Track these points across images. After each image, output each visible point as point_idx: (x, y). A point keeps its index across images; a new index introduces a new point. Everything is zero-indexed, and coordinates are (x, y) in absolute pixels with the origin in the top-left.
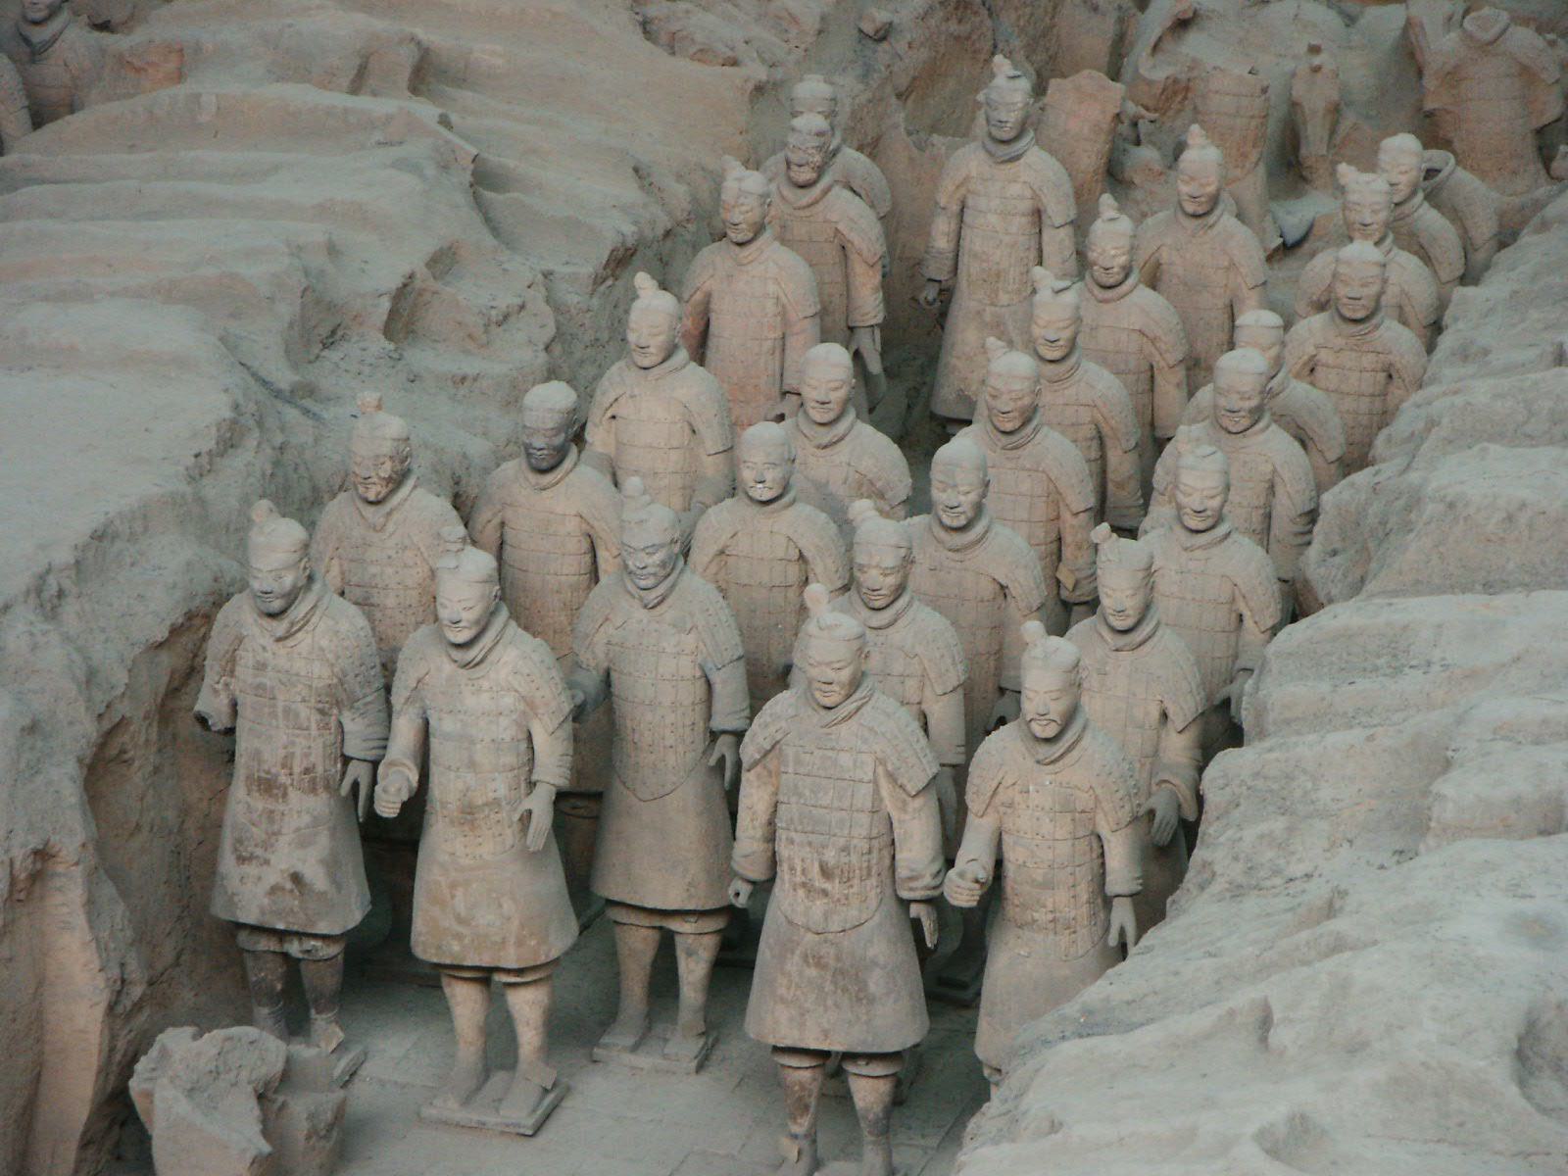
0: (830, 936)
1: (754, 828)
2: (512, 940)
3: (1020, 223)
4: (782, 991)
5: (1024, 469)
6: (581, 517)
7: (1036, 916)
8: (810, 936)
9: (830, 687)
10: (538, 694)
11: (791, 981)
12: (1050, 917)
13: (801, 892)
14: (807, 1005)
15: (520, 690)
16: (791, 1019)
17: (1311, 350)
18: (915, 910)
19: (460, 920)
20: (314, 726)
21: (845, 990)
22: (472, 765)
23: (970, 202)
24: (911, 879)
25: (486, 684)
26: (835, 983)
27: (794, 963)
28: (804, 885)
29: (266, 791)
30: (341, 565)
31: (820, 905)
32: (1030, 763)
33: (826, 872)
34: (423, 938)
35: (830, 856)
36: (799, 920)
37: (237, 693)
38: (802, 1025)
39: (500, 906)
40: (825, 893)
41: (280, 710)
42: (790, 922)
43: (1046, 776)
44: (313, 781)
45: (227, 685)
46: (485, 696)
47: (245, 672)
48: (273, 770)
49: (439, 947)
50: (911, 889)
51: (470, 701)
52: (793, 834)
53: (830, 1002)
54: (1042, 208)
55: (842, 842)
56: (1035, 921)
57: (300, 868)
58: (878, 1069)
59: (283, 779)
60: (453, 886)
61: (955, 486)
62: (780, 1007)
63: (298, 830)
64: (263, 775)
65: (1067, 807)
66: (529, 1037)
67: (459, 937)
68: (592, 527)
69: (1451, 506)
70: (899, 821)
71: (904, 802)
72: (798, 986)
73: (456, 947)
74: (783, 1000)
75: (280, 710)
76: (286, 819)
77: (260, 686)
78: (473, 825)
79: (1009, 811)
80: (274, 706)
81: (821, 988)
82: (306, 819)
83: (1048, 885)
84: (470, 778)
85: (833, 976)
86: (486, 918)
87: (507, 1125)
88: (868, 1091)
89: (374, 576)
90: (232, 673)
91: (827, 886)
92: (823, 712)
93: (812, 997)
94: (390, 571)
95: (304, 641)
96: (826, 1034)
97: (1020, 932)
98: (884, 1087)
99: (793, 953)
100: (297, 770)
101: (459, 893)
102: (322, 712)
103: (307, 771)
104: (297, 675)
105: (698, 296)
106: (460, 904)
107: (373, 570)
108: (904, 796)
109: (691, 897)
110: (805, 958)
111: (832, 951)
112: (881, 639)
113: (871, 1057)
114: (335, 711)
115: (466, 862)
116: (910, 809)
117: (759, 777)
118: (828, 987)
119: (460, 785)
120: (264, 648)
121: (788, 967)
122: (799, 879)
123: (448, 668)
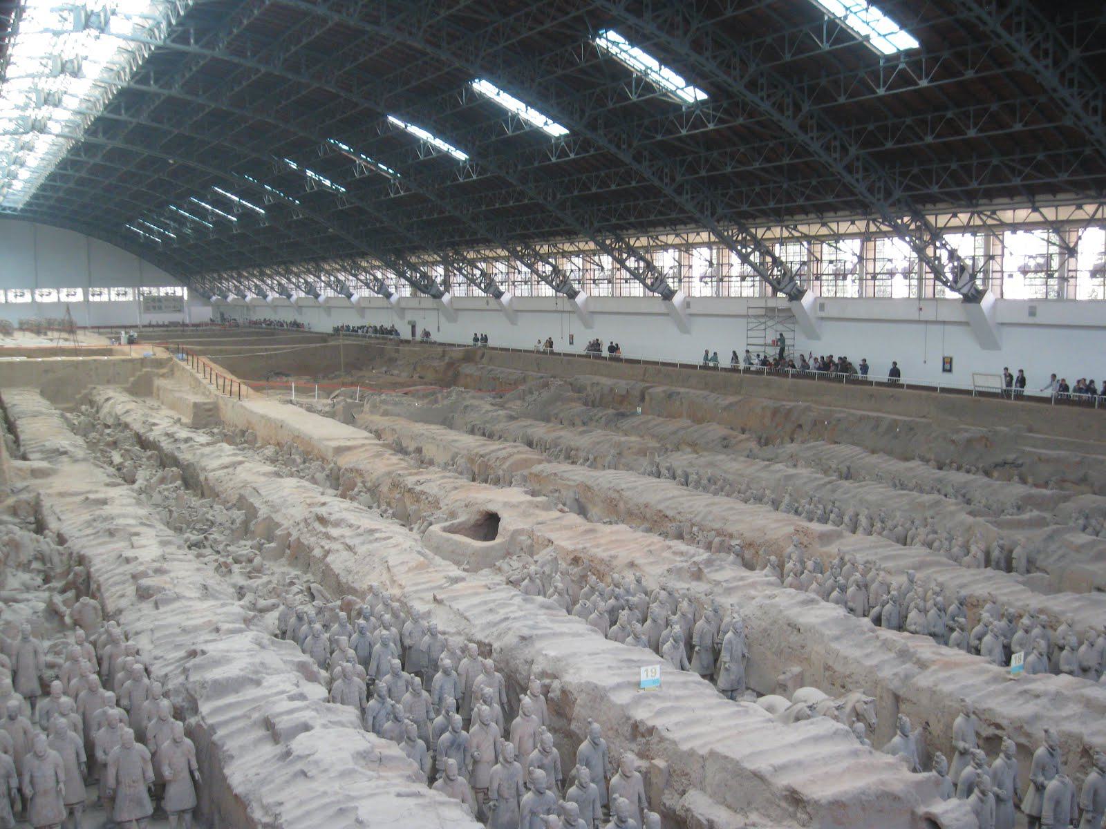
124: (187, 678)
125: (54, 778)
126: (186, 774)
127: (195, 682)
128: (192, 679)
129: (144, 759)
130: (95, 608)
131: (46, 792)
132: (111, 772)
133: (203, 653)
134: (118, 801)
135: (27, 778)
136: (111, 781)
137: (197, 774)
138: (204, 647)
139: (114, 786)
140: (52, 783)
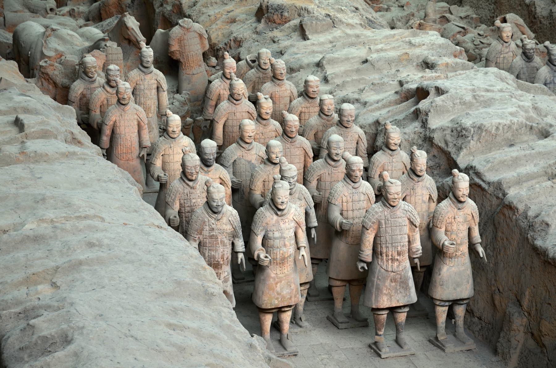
0: (398, 272)
1: (370, 246)
2: (293, 296)
3: (154, 91)
4: (385, 292)
5: (297, 147)
6: (220, 178)
7: (457, 253)
8: (393, 273)
9: (396, 200)
10: (301, 220)
11: (387, 288)
12: (461, 253)
13: (390, 261)
14: (393, 294)
15: (297, 220)
16: (387, 300)
17: (300, 109)
18: (417, 261)
19: (278, 294)
20: (228, 245)
21: (403, 287)
22: (285, 245)
23: (138, 87)
24: (417, 251)
25: (287, 220)
26: (400, 286)
27: (388, 283)
28: (392, 259)
29: (216, 267)
30: (180, 202)
31: (396, 264)
32: (456, 210)
33: (399, 254)
34: (265, 302)
35: (399, 249)
36: (390, 269)
37: (202, 240)
38: (391, 301)
39: (291, 286)
40: (397, 259)
41: (219, 242)
42: (387, 271)
43: (461, 213)
44: (228, 262)
45: (199, 238)
46: (287, 224)
47: (206, 233)
48: (219, 260)
49: (271, 304)
50: (417, 254)
51: (283, 226)
52: (387, 245)
53: (399, 292)
54: (159, 86)
55: (402, 244)
56: (456, 255)
57: (225, 289)
58: (407, 309)
59: (222, 262)
60: (277, 284)
61: (340, 148)
62: (384, 296)
63: (225, 277)
64: (215, 262)
65: (465, 221)
66: (286, 326)
67: (277, 299)
68: (223, 180)
69: (479, 128)
70: (412, 235)
71: (414, 230)
72: (389, 289)
73: (276, 302)
74: (385, 294)
75: (219, 242)
76: (221, 275)
77: (213, 235)
78: (283, 264)
79: (450, 225)
80: (218, 241)
81: (396, 288)
82: (226, 273)
83: (461, 244)
84: (285, 249)
85: (400, 284)
86: (285, 292)
87: (291, 353)
88: (402, 317)
89: (195, 203)
90: (201, 234)
91: (398, 258)
92: (391, 208)
93: (393, 291)
94: (199, 200)
95: (225, 220)
96: (398, 301)
97: (451, 259)
98: (405, 314)
99: (387, 280)
100: (225, 259)
101: (278, 285)
102: (230, 240)
103: (227, 258)
104: (224, 230)
105: (112, 123)
106: (278, 289)
107: (194, 201)
108: (414, 227)
109: (307, 278)
110: (391, 281)
111: (399, 276)
112: (357, 191)
113: (404, 306)
114: (232, 239)
115: (280, 275)
116: (416, 231)
117: (371, 231)
118: (398, 287)
119: (281, 252)
120: (213, 224)
121: (386, 284)
122: (390, 257)
123: (275, 217)
124: (424, 124)
125: (293, 241)
126: (465, 248)
127: (443, 129)
128: (434, 122)
129: (412, 223)
130: (201, 36)
131: (283, 261)
132: (369, 238)
133: (439, 91)
134: (375, 280)
135: (258, 240)
136: (367, 253)
137: (480, 250)
138: (440, 83)
139: (369, 259)
140: (291, 250)
